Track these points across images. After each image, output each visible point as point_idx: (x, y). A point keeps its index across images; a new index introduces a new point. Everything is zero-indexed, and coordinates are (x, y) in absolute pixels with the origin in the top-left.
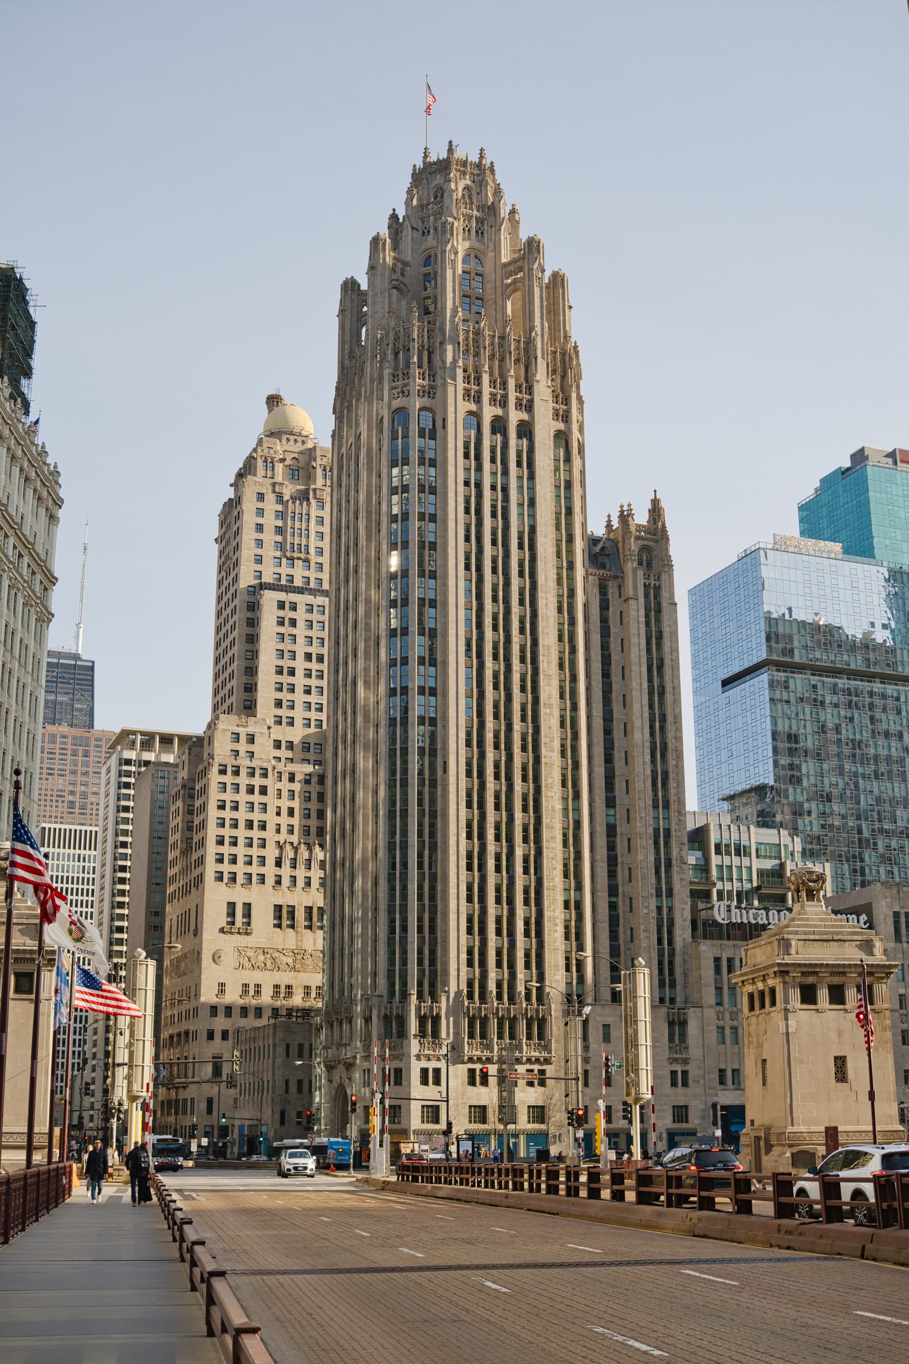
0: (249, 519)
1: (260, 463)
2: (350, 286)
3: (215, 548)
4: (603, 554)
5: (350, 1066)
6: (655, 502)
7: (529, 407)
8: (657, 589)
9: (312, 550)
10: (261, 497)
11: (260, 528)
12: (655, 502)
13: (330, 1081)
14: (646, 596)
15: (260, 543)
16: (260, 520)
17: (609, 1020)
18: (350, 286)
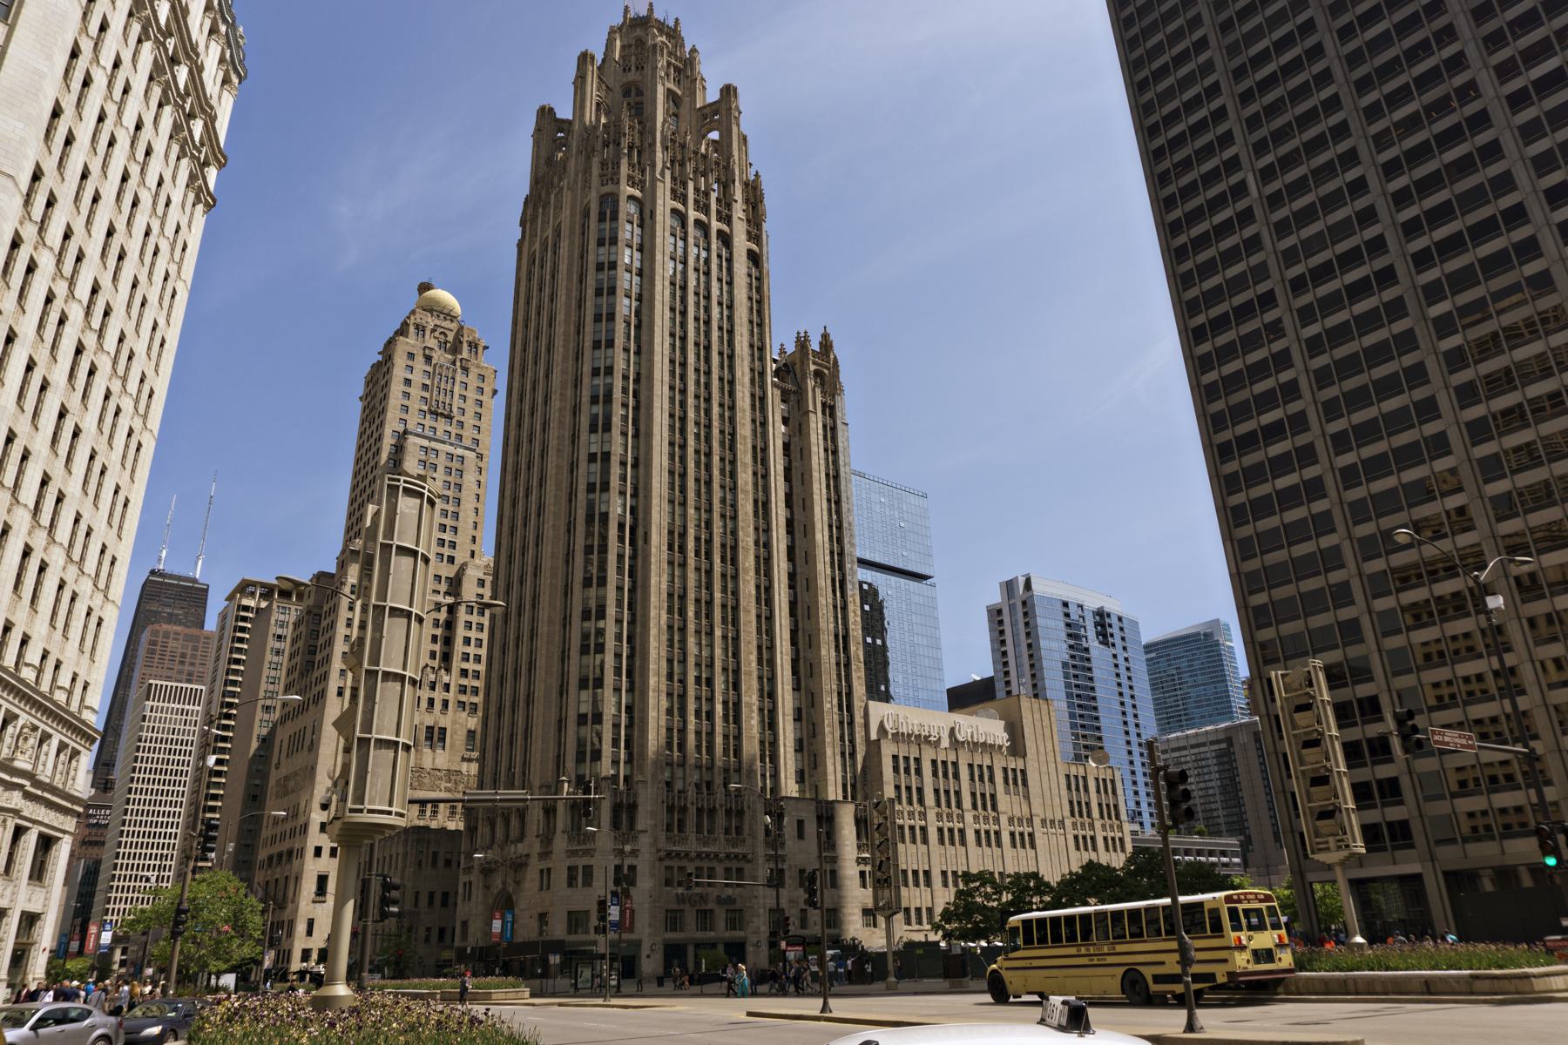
0: (399, 372)
1: (412, 329)
2: (546, 113)
3: (359, 406)
4: (786, 370)
5: (519, 865)
6: (825, 336)
7: (728, 220)
8: (832, 408)
9: (455, 409)
10: (411, 356)
11: (408, 382)
12: (825, 336)
13: (487, 887)
14: (824, 413)
15: (407, 395)
16: (409, 376)
17: (804, 815)
18: (546, 113)
